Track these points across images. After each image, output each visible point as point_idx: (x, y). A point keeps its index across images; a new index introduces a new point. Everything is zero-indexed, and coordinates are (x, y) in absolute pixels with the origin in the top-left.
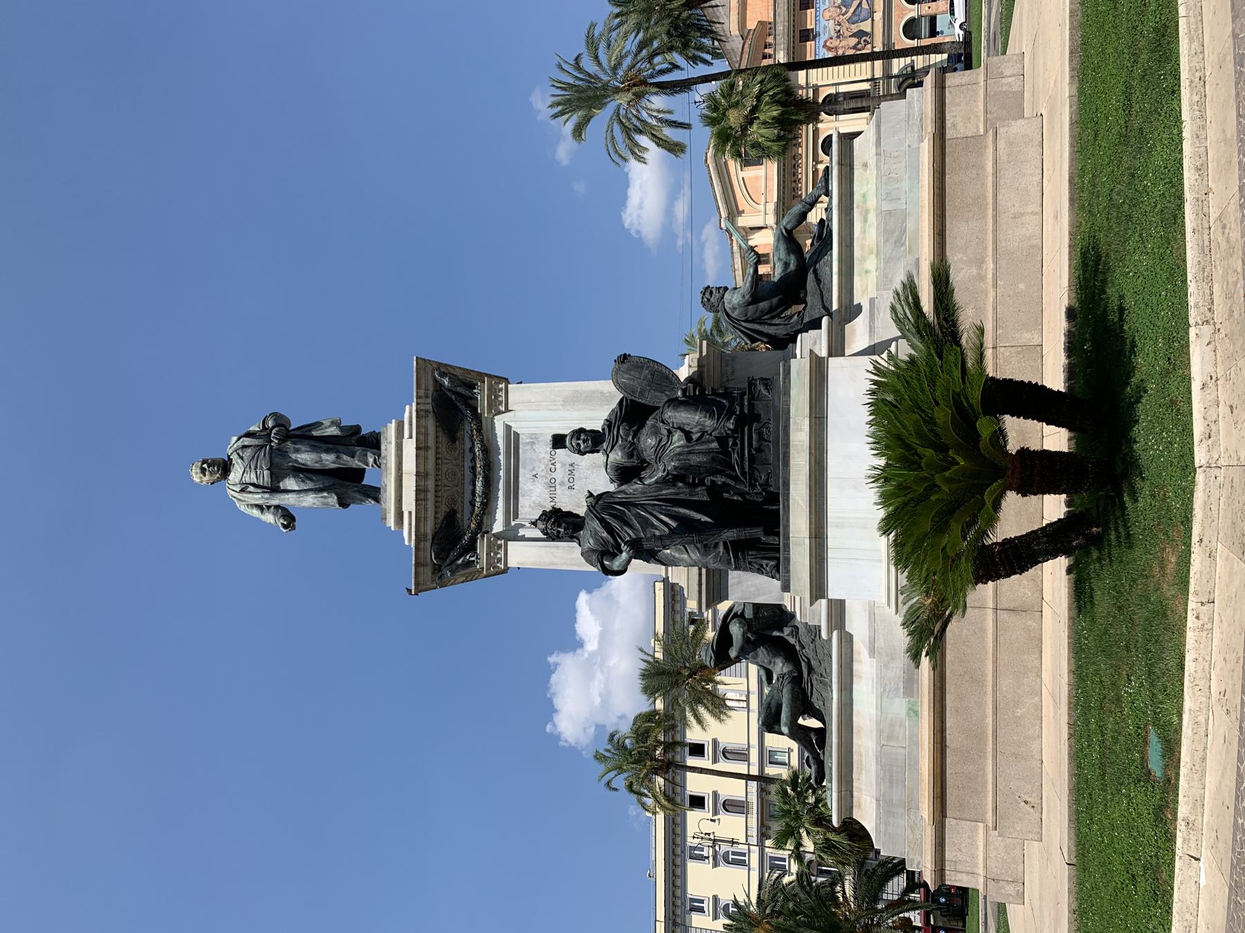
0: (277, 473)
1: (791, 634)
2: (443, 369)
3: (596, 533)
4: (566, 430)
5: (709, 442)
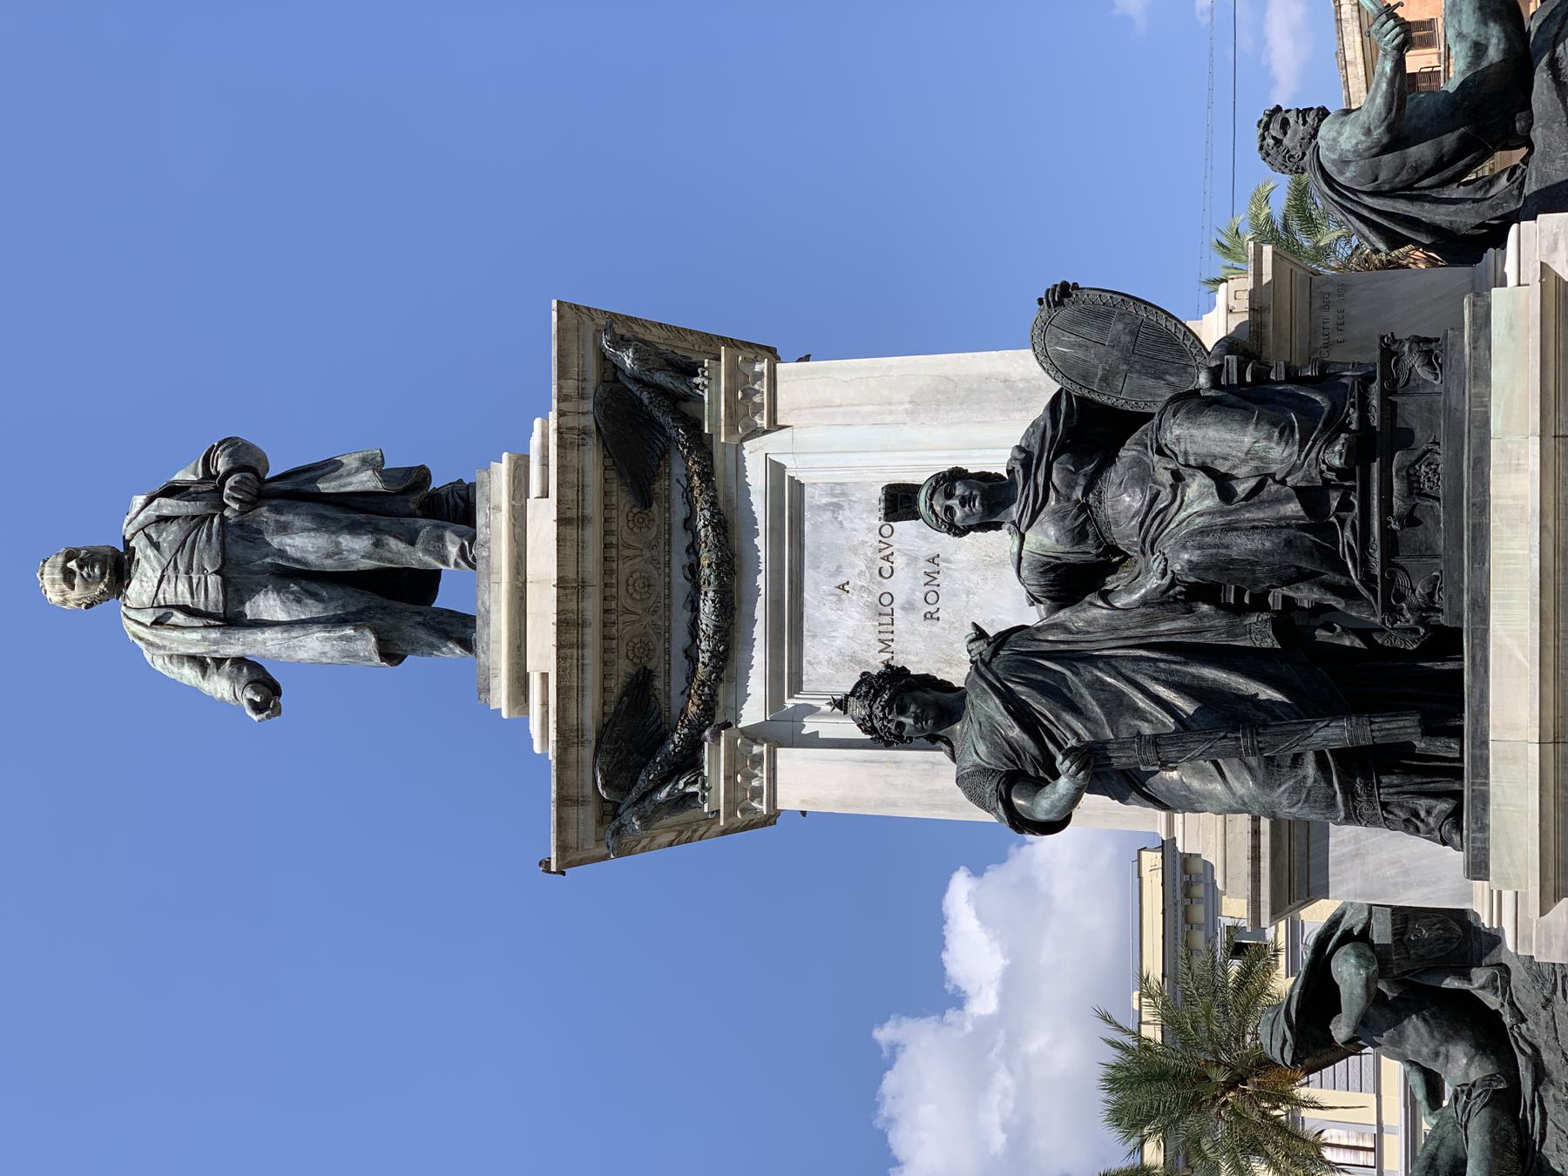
0: (239, 580)
1: (1491, 985)
2: (621, 330)
3: (994, 728)
4: (917, 474)
5: (1277, 500)
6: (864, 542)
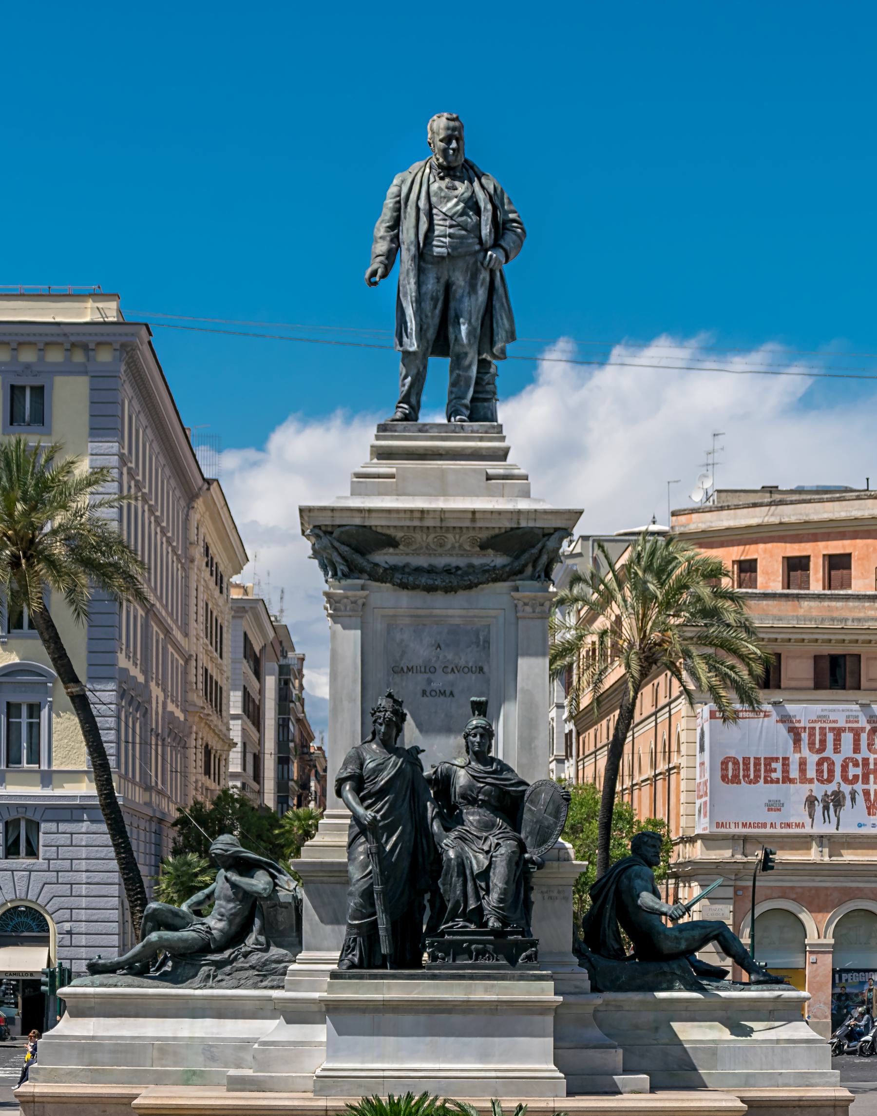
1: (257, 942)
6: (460, 659)
